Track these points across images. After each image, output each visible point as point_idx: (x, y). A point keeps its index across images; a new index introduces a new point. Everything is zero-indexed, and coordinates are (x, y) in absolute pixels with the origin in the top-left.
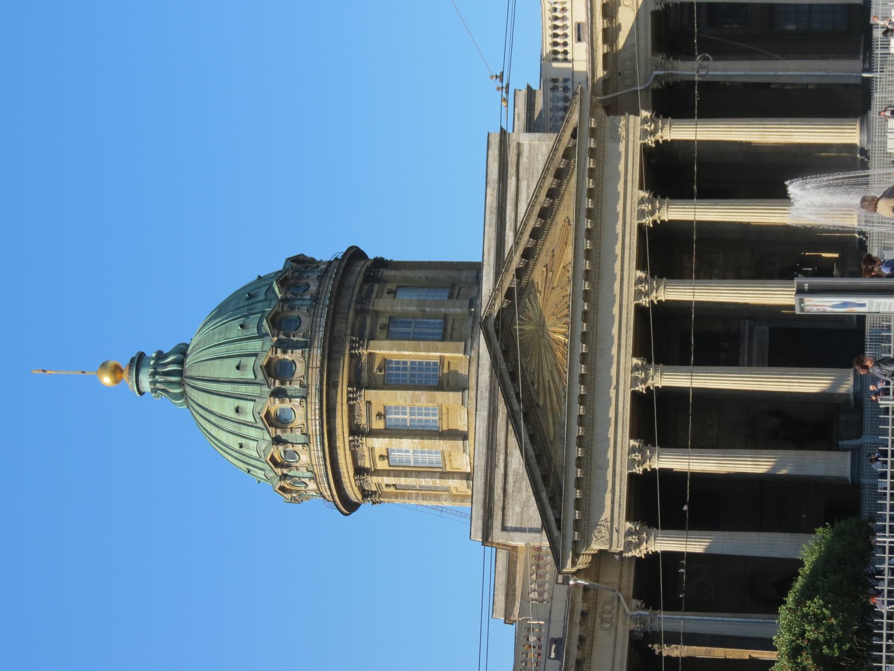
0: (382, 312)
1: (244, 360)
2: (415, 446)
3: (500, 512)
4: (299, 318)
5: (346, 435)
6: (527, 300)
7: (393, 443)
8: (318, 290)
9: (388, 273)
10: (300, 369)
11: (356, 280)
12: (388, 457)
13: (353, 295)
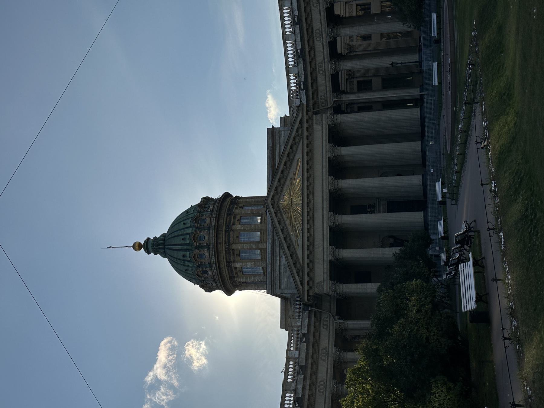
1: (185, 236)
2: (252, 266)
3: (278, 281)
5: (225, 263)
7: (244, 265)
9: (239, 200)
10: (207, 238)
11: (228, 204)
13: (226, 208)
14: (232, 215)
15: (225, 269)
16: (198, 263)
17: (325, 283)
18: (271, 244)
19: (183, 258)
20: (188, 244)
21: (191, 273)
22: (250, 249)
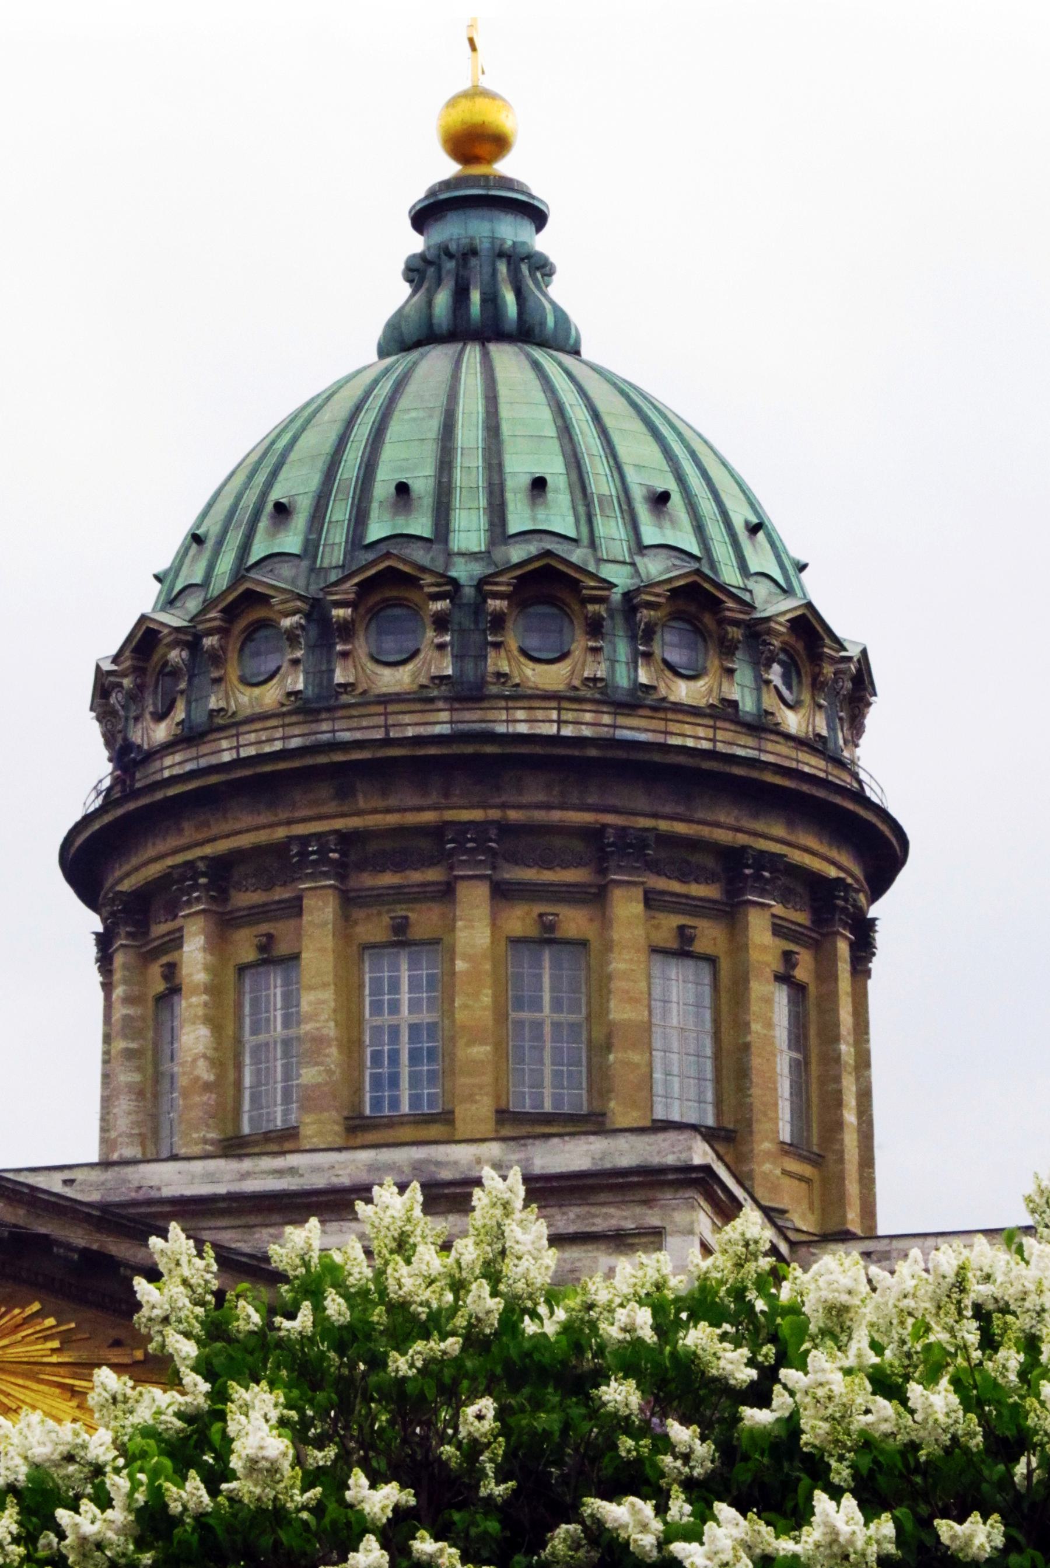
0: (604, 915)
4: (563, 656)
5: (208, 850)
6: (36, 1306)
8: (679, 708)
11: (717, 825)
13: (655, 816)
14: (602, 871)
15: (175, 852)
16: (209, 633)
20: (362, 536)
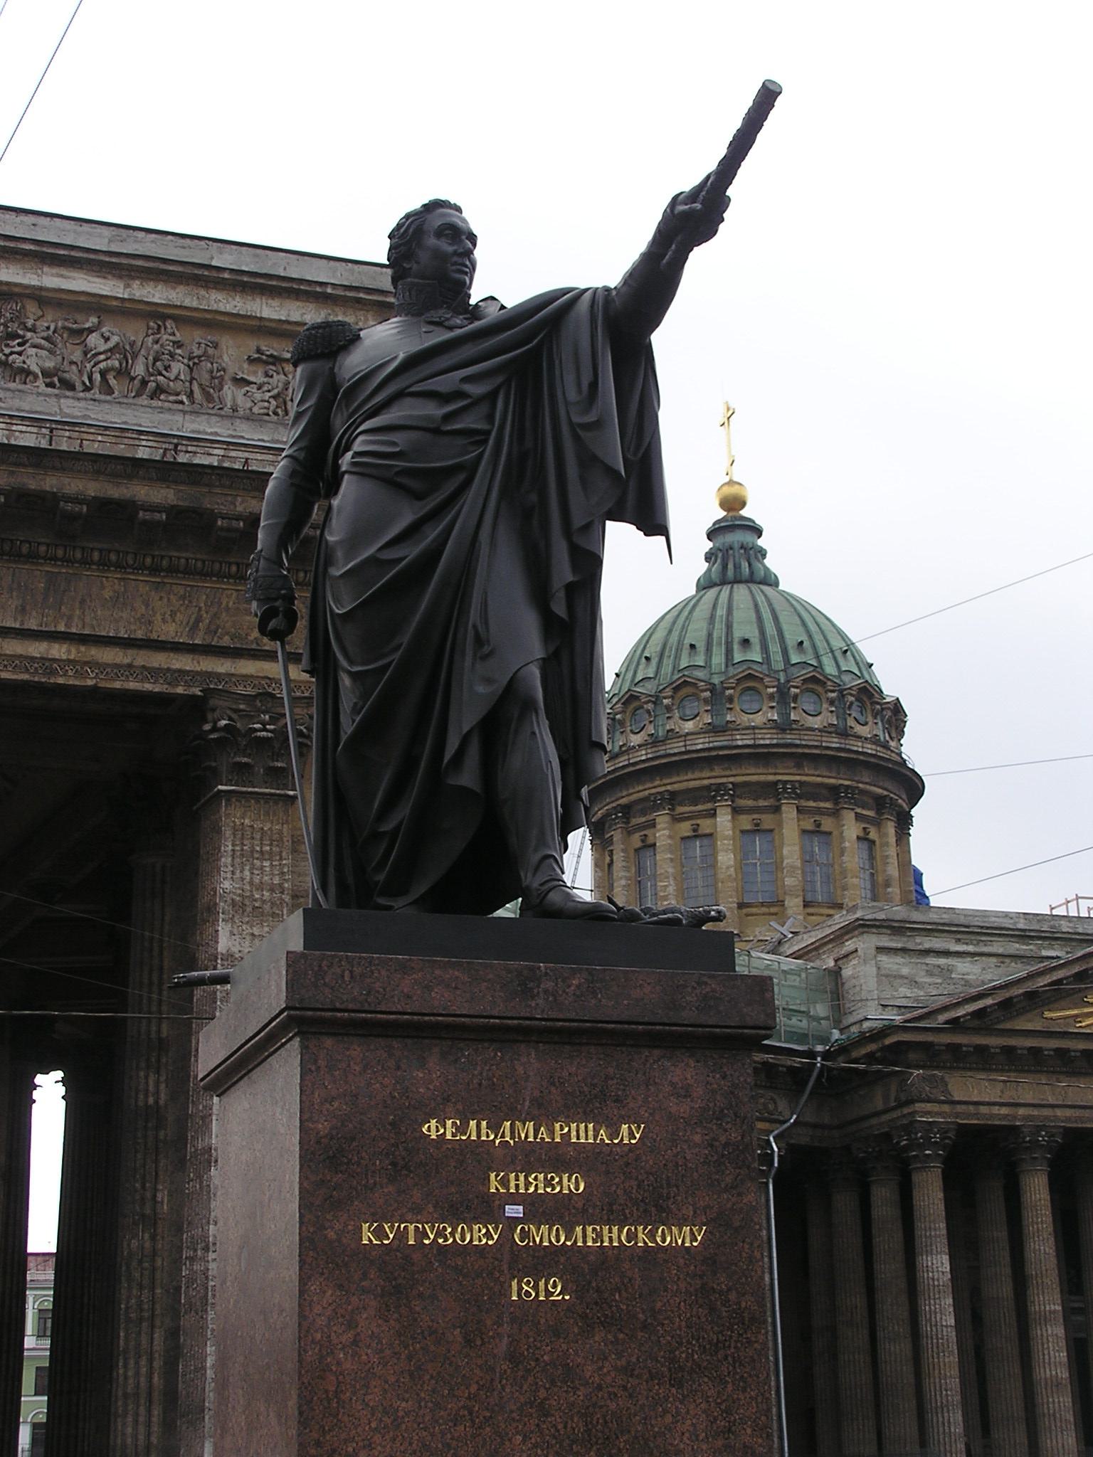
0: (880, 831)
1: (810, 651)
2: (724, 871)
3: (900, 945)
4: (866, 724)
5: (731, 779)
12: (696, 836)
13: (895, 794)
15: (709, 778)
16: (728, 688)
17: (946, 1108)
18: (1011, 927)
19: (736, 641)
21: (684, 663)
22: (778, 866)
